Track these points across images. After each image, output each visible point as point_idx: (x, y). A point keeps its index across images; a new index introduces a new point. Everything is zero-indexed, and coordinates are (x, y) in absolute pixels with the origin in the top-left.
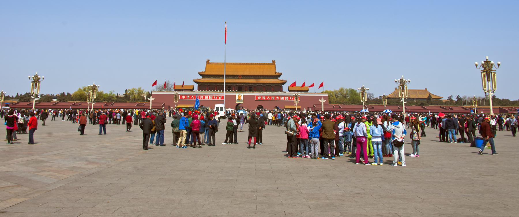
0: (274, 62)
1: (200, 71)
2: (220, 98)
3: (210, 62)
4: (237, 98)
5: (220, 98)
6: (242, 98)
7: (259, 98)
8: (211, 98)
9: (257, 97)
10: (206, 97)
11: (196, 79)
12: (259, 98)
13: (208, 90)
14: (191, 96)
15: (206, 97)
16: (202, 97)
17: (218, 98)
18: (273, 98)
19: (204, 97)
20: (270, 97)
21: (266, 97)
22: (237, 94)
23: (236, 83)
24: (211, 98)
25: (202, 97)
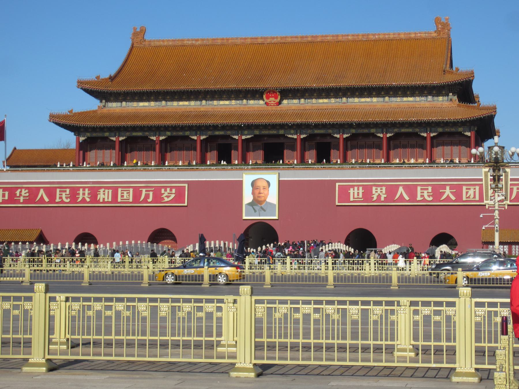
0: (444, 27)
1: (90, 76)
2: (168, 196)
3: (148, 37)
4: (248, 197)
5: (168, 196)
6: (272, 196)
7: (356, 194)
8: (127, 196)
9: (345, 192)
10: (104, 196)
11: (63, 110)
12: (356, 194)
13: (120, 163)
14: (33, 192)
15: (104, 196)
16: (84, 195)
17: (158, 197)
18: (424, 195)
19: (94, 192)
20: (411, 190)
21: (392, 190)
22: (248, 178)
23: (249, 127)
24: (127, 196)
25: (84, 195)
